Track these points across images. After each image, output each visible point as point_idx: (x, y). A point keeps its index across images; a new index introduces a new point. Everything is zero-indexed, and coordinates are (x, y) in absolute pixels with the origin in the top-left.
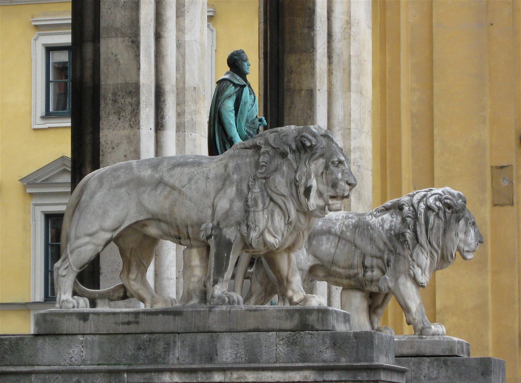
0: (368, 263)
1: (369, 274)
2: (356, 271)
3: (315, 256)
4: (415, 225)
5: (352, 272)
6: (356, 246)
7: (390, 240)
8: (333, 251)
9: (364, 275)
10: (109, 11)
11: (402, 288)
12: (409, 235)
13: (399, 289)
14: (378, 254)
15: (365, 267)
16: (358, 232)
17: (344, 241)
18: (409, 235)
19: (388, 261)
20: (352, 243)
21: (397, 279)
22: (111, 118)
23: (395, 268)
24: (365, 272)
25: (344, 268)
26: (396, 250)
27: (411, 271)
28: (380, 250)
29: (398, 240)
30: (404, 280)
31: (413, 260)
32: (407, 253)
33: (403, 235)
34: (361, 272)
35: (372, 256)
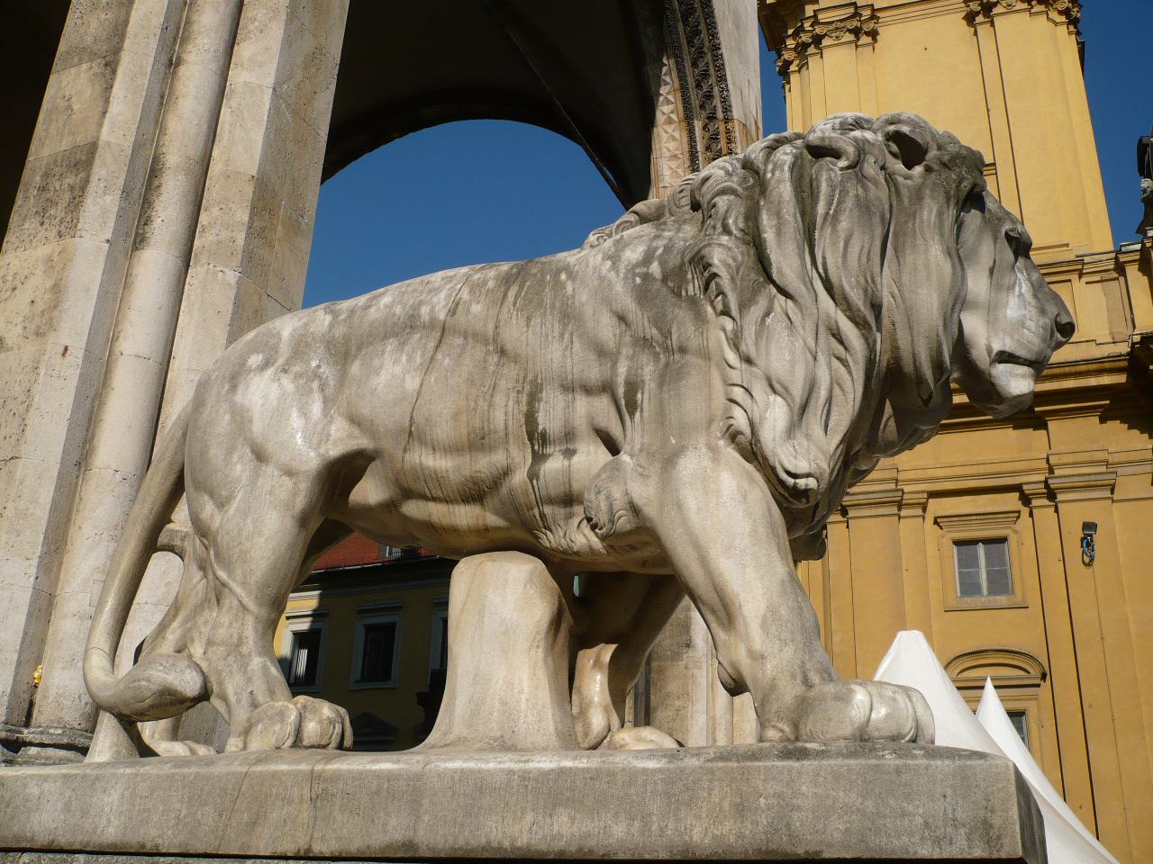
0: (550, 417)
1: (554, 464)
2: (498, 459)
3: (354, 420)
4: (752, 217)
5: (484, 464)
6: (502, 352)
7: (643, 295)
8: (412, 383)
9: (533, 475)
10: (79, 21)
11: (692, 501)
12: (724, 254)
13: (679, 506)
14: (594, 373)
15: (538, 440)
16: (516, 297)
17: (459, 341)
18: (724, 254)
19: (633, 387)
20: (486, 342)
21: (669, 461)
22: (27, 226)
23: (661, 416)
24: (538, 458)
25: (453, 449)
26: (667, 335)
27: (738, 413)
28: (601, 352)
29: (679, 295)
30: (707, 463)
31: (748, 360)
32: (718, 332)
33: (700, 262)
34: (520, 458)
35: (568, 388)
